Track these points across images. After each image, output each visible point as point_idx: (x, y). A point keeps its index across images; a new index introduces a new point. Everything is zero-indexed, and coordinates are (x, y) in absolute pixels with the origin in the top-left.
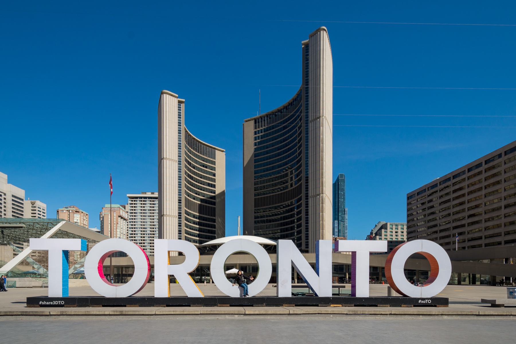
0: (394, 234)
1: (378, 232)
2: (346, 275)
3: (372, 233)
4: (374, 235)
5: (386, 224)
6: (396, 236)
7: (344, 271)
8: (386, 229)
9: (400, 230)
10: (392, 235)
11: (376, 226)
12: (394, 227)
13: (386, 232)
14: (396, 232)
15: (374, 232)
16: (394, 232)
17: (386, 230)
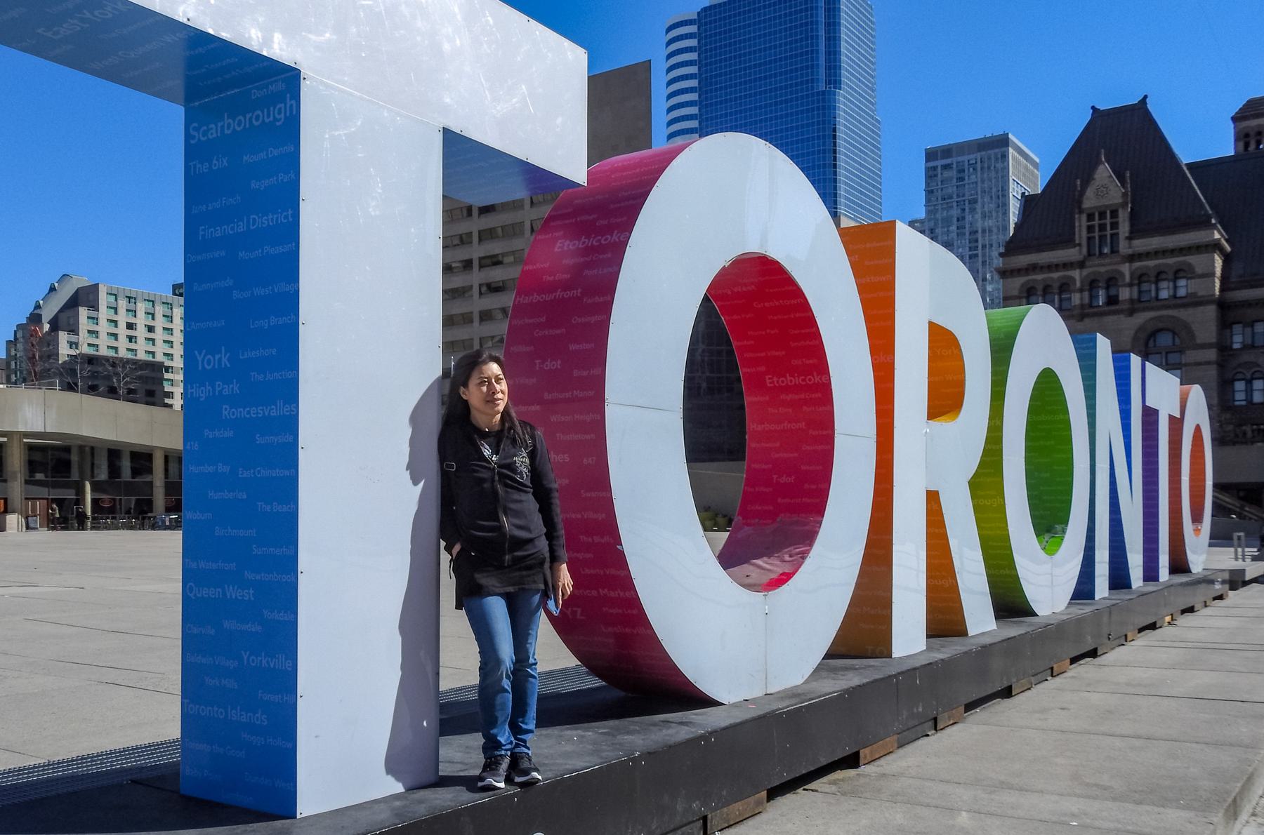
0: (122, 331)
1: (63, 317)
2: (80, 491)
3: (35, 318)
4: (47, 327)
5: (94, 289)
6: (130, 338)
7: (75, 476)
8: (94, 306)
9: (141, 321)
10: (115, 336)
11: (52, 289)
12: (123, 304)
13: (95, 320)
14: (130, 326)
15: (48, 314)
16: (122, 325)
17: (93, 314)
